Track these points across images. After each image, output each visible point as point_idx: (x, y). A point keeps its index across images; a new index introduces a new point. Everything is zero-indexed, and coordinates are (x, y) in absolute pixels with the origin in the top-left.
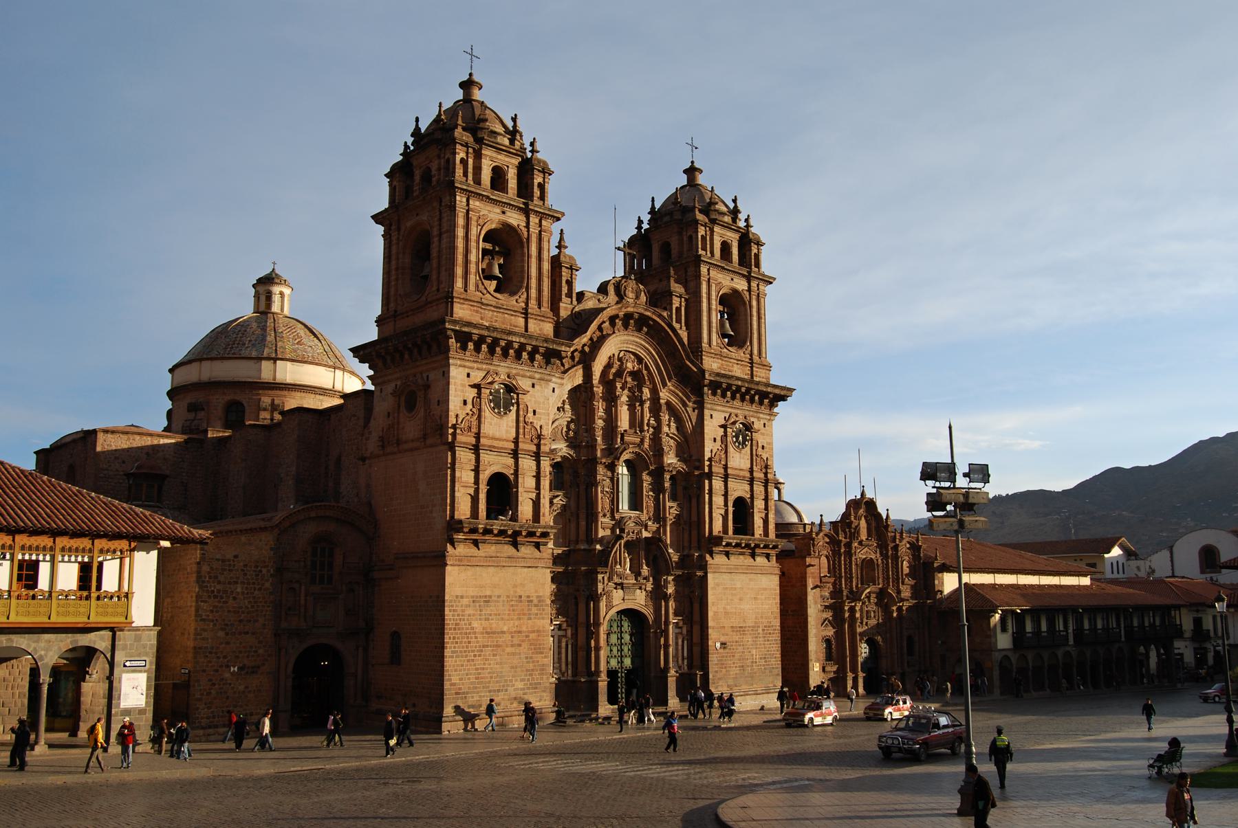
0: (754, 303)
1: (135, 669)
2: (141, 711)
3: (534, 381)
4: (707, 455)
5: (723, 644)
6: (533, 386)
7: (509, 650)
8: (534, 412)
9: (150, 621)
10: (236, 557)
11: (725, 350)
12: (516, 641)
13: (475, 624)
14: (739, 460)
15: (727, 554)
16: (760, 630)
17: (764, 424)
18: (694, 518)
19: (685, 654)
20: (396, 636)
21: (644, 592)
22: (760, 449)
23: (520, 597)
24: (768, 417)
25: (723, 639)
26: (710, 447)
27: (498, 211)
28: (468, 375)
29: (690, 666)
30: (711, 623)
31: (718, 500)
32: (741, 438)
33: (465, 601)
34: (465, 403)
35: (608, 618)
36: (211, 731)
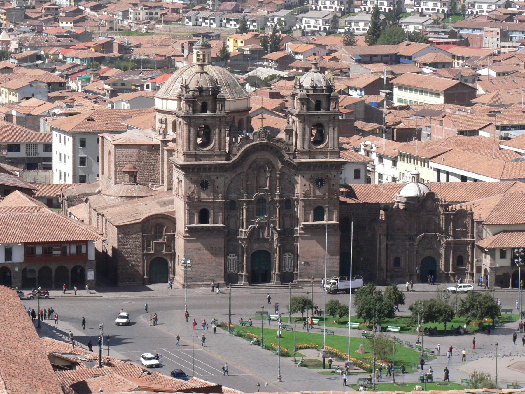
2: (93, 280)
5: (307, 264)
6: (217, 178)
7: (208, 264)
8: (218, 187)
9: (94, 259)
10: (129, 232)
12: (210, 262)
13: (195, 257)
17: (335, 176)
19: (292, 265)
20: (178, 256)
21: (268, 244)
22: (332, 186)
24: (337, 173)
25: (306, 260)
27: (203, 120)
32: (320, 183)
33: (191, 250)
35: (251, 253)
36: (124, 283)
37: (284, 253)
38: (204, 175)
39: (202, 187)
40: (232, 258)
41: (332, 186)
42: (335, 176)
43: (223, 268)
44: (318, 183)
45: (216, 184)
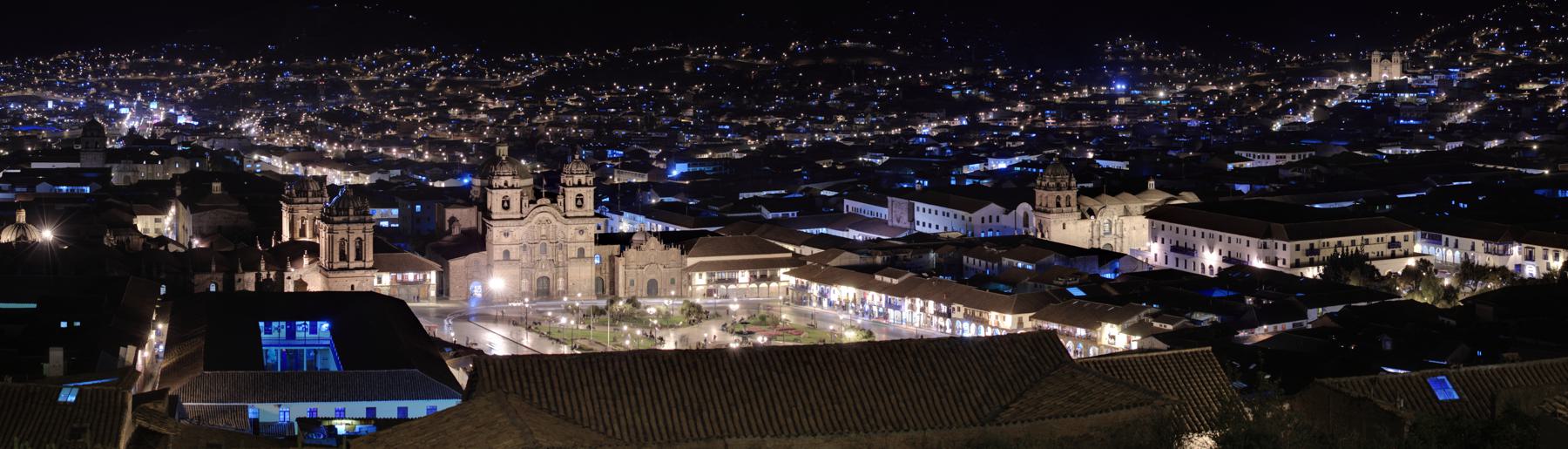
26: (569, 236)
38: (506, 228)
39: (505, 234)
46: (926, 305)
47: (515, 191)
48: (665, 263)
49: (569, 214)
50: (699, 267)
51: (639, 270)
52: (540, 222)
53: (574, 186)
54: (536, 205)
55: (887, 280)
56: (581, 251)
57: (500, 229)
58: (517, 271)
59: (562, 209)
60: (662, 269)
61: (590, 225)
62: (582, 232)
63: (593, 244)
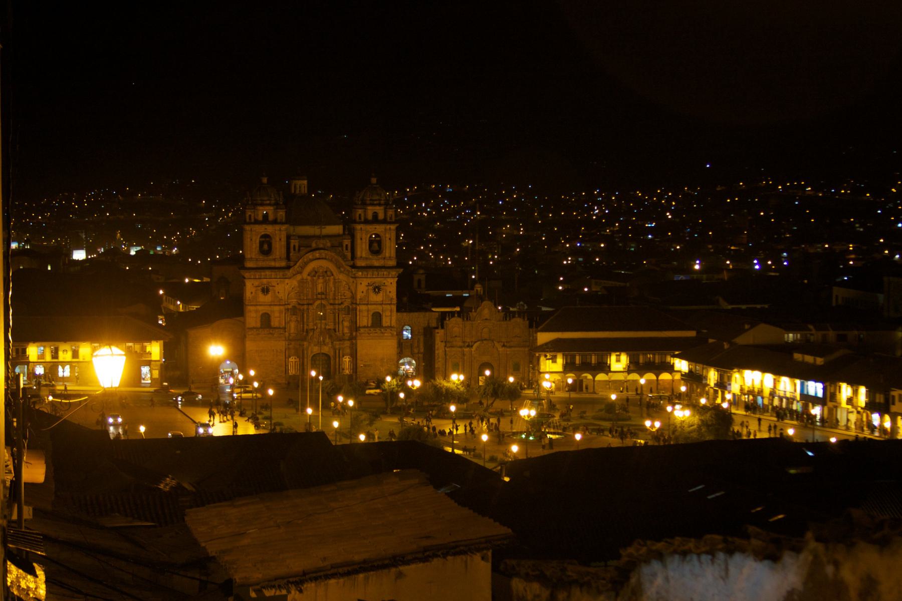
0: (388, 236)
1: (155, 369)
2: (157, 379)
3: (278, 282)
4: (358, 297)
6: (278, 284)
11: (371, 256)
14: (374, 298)
15: (368, 333)
16: (385, 360)
17: (391, 283)
18: (355, 321)
23: (273, 350)
26: (359, 296)
28: (253, 284)
29: (353, 372)
30: (358, 358)
31: (365, 314)
32: (377, 290)
34: (252, 293)
37: (343, 356)
38: (265, 281)
40: (293, 360)
41: (388, 293)
42: (391, 283)
43: (284, 369)
44: (375, 290)
45: (277, 288)
46: (856, 392)
47: (277, 227)
48: (503, 340)
49: (360, 263)
50: (554, 348)
51: (467, 350)
52: (314, 273)
53: (366, 222)
54: (308, 249)
55: (809, 359)
56: (377, 319)
57: (256, 283)
58: (281, 345)
59: (349, 255)
60: (501, 349)
61: (389, 280)
62: (377, 289)
63: (394, 308)
